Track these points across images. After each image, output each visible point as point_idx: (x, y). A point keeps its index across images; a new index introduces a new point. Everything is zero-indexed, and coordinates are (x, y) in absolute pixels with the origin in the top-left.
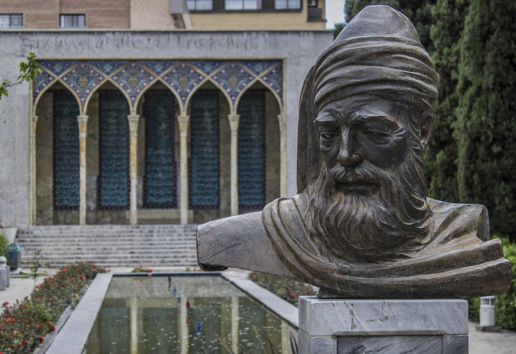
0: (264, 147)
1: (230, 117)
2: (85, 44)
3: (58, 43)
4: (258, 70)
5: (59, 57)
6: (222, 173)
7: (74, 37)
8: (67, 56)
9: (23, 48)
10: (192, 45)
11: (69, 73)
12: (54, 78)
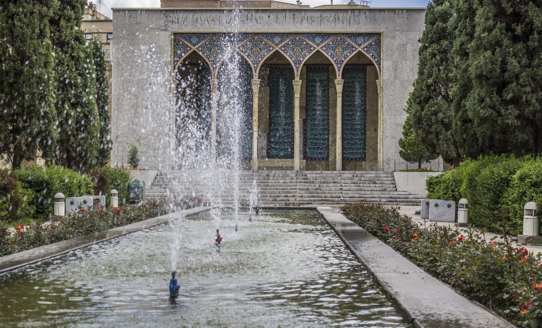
0: (365, 111)
1: (336, 82)
2: (216, 20)
3: (195, 20)
4: (359, 42)
5: (195, 30)
6: (331, 132)
7: (208, 14)
8: (201, 30)
9: (166, 23)
10: (305, 21)
11: (203, 44)
12: (191, 48)
